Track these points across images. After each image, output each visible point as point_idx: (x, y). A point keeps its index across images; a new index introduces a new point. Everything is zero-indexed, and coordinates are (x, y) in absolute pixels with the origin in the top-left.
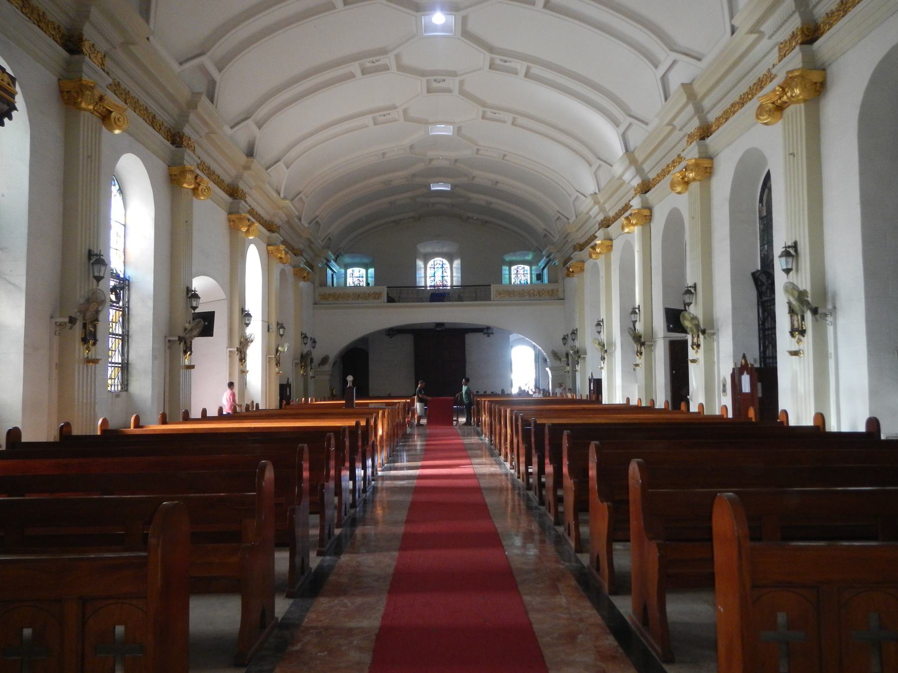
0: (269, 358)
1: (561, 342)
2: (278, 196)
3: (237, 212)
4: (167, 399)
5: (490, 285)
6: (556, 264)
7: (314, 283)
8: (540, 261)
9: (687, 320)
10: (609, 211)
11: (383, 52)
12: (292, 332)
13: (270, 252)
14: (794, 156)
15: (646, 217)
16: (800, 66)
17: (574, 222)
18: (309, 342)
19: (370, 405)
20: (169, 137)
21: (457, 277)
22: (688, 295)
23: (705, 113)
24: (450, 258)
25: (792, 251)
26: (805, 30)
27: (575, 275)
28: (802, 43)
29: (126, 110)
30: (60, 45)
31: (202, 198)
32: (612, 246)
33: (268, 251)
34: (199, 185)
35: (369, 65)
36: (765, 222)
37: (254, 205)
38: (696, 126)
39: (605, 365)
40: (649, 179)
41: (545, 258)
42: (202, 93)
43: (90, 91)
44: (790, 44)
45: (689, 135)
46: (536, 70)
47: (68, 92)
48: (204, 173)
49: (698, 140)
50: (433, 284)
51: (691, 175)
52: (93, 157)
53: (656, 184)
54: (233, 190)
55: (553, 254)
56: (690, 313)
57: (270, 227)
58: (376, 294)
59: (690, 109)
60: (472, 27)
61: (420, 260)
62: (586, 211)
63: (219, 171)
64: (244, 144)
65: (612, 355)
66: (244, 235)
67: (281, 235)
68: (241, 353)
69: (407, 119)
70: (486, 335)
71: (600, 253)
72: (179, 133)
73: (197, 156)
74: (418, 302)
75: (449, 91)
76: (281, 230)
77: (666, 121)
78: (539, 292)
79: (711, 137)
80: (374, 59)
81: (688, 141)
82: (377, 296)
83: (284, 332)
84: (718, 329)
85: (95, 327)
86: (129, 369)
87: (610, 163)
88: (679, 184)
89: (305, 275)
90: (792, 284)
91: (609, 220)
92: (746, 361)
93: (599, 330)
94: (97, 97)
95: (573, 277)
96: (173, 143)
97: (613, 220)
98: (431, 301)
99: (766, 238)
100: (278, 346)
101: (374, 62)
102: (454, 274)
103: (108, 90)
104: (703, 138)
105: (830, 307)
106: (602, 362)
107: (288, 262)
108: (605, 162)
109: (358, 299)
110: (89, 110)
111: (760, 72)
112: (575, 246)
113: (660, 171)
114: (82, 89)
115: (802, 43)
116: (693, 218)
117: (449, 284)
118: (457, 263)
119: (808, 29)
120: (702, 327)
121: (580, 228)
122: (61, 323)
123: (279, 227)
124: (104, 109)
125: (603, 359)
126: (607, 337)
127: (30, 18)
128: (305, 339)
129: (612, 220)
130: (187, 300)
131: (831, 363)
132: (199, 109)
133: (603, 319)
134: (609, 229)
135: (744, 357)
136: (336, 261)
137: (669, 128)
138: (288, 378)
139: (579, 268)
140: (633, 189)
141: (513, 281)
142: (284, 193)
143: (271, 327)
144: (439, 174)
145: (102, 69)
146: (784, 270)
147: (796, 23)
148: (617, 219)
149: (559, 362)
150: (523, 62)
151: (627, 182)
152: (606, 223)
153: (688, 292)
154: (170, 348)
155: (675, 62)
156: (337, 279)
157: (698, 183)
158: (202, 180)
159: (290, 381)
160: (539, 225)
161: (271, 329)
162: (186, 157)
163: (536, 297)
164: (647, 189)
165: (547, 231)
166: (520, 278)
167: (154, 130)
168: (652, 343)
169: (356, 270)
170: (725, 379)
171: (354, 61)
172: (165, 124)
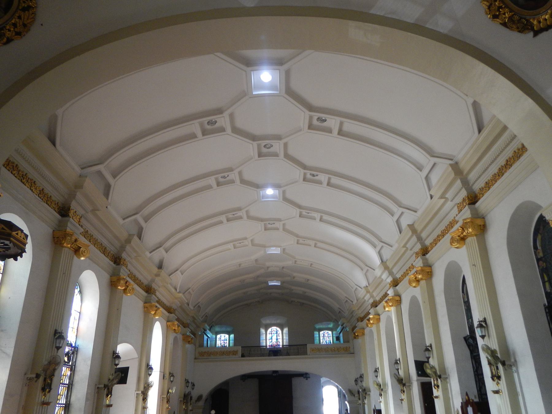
0: (163, 397)
1: (354, 383)
3: (150, 302)
5: (306, 345)
6: (348, 330)
7: (195, 345)
8: (338, 328)
9: (428, 369)
10: (376, 297)
12: (179, 379)
13: (169, 326)
14: (475, 266)
15: (398, 301)
16: (470, 216)
17: (356, 304)
18: (190, 385)
20: (113, 259)
21: (287, 339)
25: (484, 324)
26: (470, 197)
28: (469, 204)
29: (89, 246)
30: (57, 213)
31: (129, 295)
32: (380, 319)
33: (167, 325)
34: (128, 287)
36: (467, 305)
39: (382, 399)
41: (340, 326)
42: (135, 234)
43: (70, 237)
44: (463, 204)
45: (416, 253)
46: (325, 217)
47: (57, 238)
48: (131, 279)
49: (421, 256)
50: (271, 344)
51: (420, 277)
52: (66, 274)
53: (401, 281)
54: (148, 289)
55: (345, 324)
56: (429, 364)
57: (169, 310)
59: (414, 239)
60: (289, 196)
61: (263, 328)
62: (362, 297)
63: (140, 277)
64: (157, 260)
65: (386, 392)
66: (153, 316)
67: (176, 315)
68: (144, 394)
69: (253, 245)
70: (305, 378)
71: (373, 324)
72: (119, 257)
73: (128, 270)
74: (261, 356)
75: (277, 229)
76: (176, 312)
77: (402, 245)
80: (234, 213)
83: (173, 379)
84: (449, 375)
85: (51, 380)
86: (70, 408)
87: (373, 268)
88: (414, 281)
89: (190, 340)
90: (486, 345)
92: (468, 397)
93: (377, 375)
94: (73, 240)
95: (358, 338)
96: (114, 263)
97: (379, 303)
98: (269, 356)
100: (169, 389)
101: (234, 215)
102: (284, 338)
103: (80, 235)
104: (424, 255)
105: (513, 360)
106: (380, 397)
107: (180, 332)
109: (223, 355)
110: (68, 247)
111: (450, 218)
114: (65, 235)
115: (469, 204)
117: (281, 344)
118: (286, 330)
119: (471, 196)
120: (438, 373)
121: (361, 307)
122: (30, 378)
123: (175, 310)
124: (77, 246)
125: (381, 395)
126: (382, 380)
127: (42, 200)
128: (188, 383)
129: (378, 303)
131: (520, 398)
132: (132, 243)
133: (378, 368)
135: (467, 394)
136: (210, 330)
137: (405, 249)
138: (174, 412)
139: (361, 333)
141: (321, 341)
143: (165, 376)
144: (274, 275)
145: (79, 224)
146: (480, 336)
147: (464, 193)
148: (381, 302)
149: (353, 397)
150: (318, 213)
152: (375, 305)
153: (427, 350)
154: (98, 393)
155: (402, 213)
157: (424, 281)
158: (130, 283)
160: (336, 306)
161: (165, 377)
162: (122, 270)
164: (396, 284)
165: (340, 309)
166: (326, 340)
168: (410, 384)
169: (223, 335)
170: (458, 410)
172: (112, 252)
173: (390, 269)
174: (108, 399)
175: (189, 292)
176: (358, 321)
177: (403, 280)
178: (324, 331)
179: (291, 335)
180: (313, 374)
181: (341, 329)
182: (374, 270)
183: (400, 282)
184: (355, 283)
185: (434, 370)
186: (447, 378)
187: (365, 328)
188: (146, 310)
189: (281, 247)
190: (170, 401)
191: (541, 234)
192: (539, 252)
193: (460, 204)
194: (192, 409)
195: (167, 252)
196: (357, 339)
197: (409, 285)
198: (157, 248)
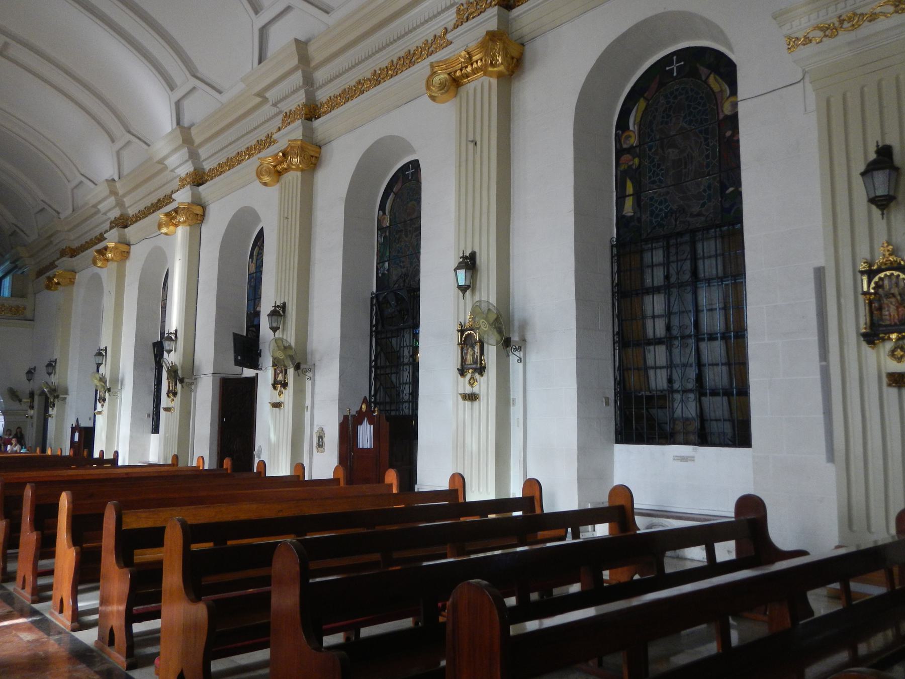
10: (128, 207)
14: (476, 144)
17: (66, 218)
22: (274, 318)
23: (315, 88)
27: (60, 288)
32: (128, 253)
36: (387, 234)
38: (300, 103)
40: (204, 169)
41: (8, 263)
49: (303, 118)
51: (296, 160)
53: (215, 176)
62: (93, 202)
71: (112, 260)
79: (318, 120)
84: (315, 364)
88: (269, 173)
91: (127, 220)
95: (56, 289)
97: (134, 220)
99: (388, 254)
112: (63, 249)
113: (224, 160)
129: (132, 220)
133: (106, 348)
134: (126, 229)
137: (259, 99)
139: (68, 280)
140: (178, 179)
146: (459, 287)
149: (18, 402)
164: (200, 182)
165: (16, 226)
168: (192, 382)
173: (195, 145)
176: (63, 253)
182: (149, 145)
183: (212, 179)
184: (79, 171)
185: (291, 353)
186: (305, 371)
187: (76, 271)
191: (646, 99)
192: (629, 137)
193: (465, 6)
197: (256, 177)
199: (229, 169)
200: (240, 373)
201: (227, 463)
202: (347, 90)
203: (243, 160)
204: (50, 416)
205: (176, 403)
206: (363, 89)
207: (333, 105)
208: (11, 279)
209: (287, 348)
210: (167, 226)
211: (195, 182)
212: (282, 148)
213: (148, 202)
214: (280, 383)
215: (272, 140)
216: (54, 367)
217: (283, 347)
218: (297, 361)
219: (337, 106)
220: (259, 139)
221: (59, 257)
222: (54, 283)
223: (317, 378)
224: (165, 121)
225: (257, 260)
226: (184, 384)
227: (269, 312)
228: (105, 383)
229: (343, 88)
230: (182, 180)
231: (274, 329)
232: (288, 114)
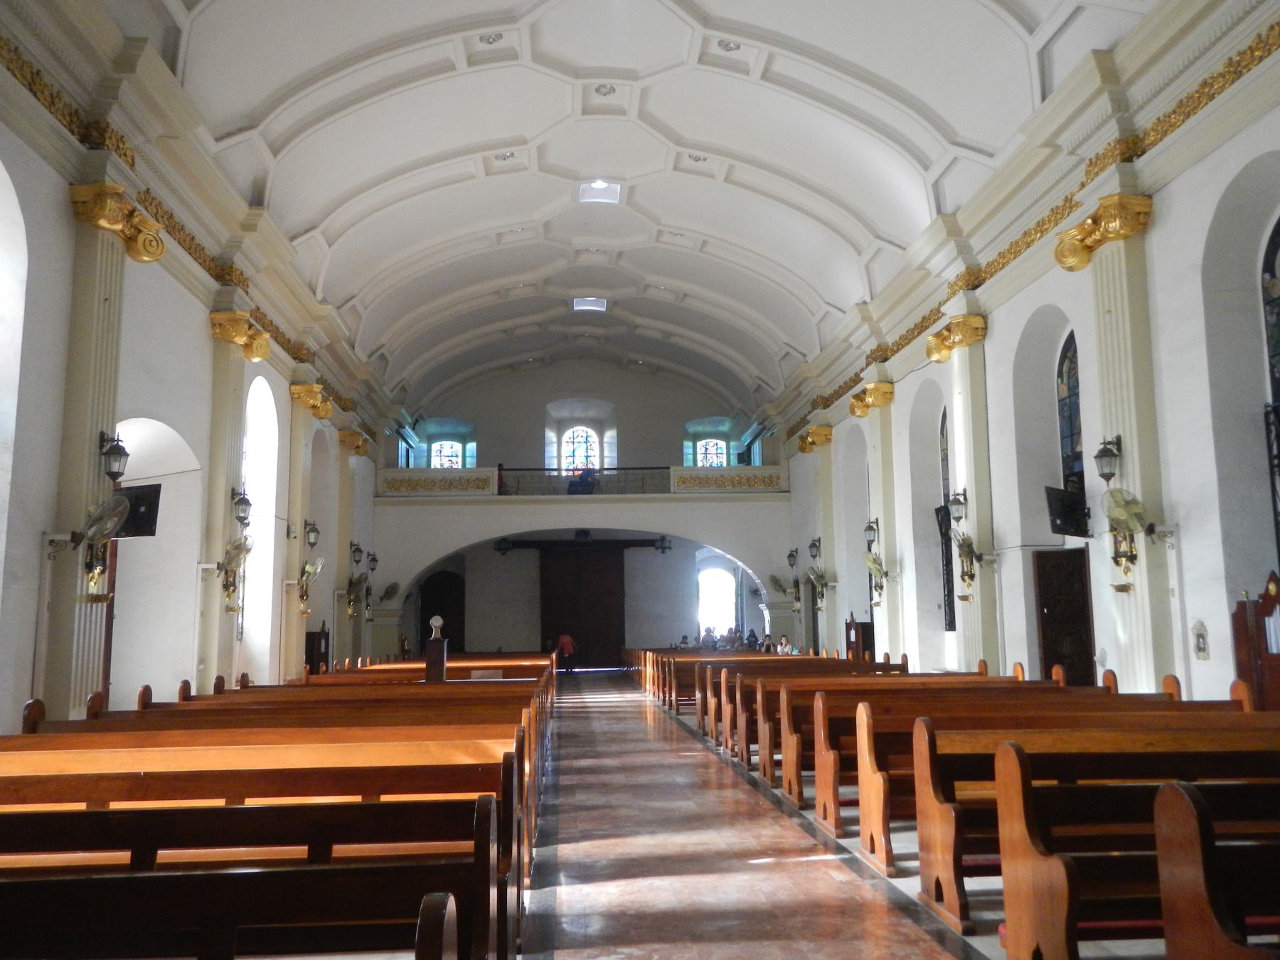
0: (288, 585)
1: (787, 562)
2: (312, 295)
3: (230, 310)
4: (42, 665)
5: (669, 468)
6: (775, 435)
7: (375, 462)
8: (743, 432)
10: (887, 333)
11: (509, 17)
13: (296, 396)
17: (816, 358)
19: (473, 673)
20: (74, 126)
22: (1106, 460)
23: (1132, 111)
24: (600, 427)
27: (815, 448)
31: (146, 258)
32: (892, 393)
33: (292, 394)
34: (140, 231)
35: (482, 47)
37: (266, 308)
40: (979, 265)
41: (755, 425)
42: (145, 40)
49: (1118, 161)
50: (571, 467)
51: (1115, 225)
53: (996, 271)
57: (298, 352)
58: (480, 480)
59: (1104, 103)
61: (552, 429)
62: (845, 334)
64: (245, 179)
66: (243, 354)
68: (226, 572)
69: (544, 168)
70: (660, 550)
71: (873, 405)
72: (97, 122)
74: (549, 493)
75: (622, 112)
76: (317, 362)
78: (748, 480)
81: (1088, 172)
82: (481, 484)
83: (317, 538)
84: (1177, 525)
88: (1074, 251)
89: (360, 443)
91: (886, 351)
96: (82, 141)
97: (895, 349)
100: (306, 564)
101: (490, 43)
102: (606, 453)
107: (330, 415)
108: (890, 242)
109: (449, 488)
112: (814, 400)
113: (1007, 246)
116: (1109, 312)
118: (610, 435)
126: (886, 548)
130: (100, 459)
132: (138, 69)
133: (877, 519)
134: (886, 363)
137: (1047, 151)
138: (324, 622)
141: (700, 464)
142: (323, 291)
143: (293, 528)
144: (589, 280)
149: (782, 594)
151: (934, 274)
152: (882, 355)
156: (415, 458)
158: (143, 221)
159: (327, 627)
160: (747, 371)
162: (110, 170)
163: (744, 487)
164: (976, 283)
166: (711, 461)
167: (36, 100)
171: (455, 32)
172: (66, 99)
174: (93, 577)
175: (354, 306)
177: (1003, 268)
178: (708, 440)
179: (623, 446)
180: (680, 538)
181: (757, 432)
182: (904, 249)
183: (991, 276)
184: (823, 299)
185: (1137, 510)
186: (1163, 536)
188: (220, 333)
189: (624, 180)
190: (309, 592)
194: (371, 618)
195: (275, 153)
196: (808, 452)
197: (1056, 262)
198: (241, 130)
199: (1015, 258)
200: (1062, 543)
201: (1057, 673)
202: (1185, 101)
203: (1033, 241)
204: (819, 609)
205: (974, 589)
206: (1212, 91)
207: (1165, 128)
208: (760, 444)
209: (1129, 503)
210: (938, 350)
211: (969, 285)
212: (1092, 211)
213: (910, 323)
214: (1124, 555)
215: (1073, 203)
216: (818, 548)
217: (1123, 503)
218: (1148, 522)
219: (1171, 129)
220: (1053, 206)
221: (810, 410)
222: (808, 443)
223: (1185, 545)
224: (921, 211)
225: (1069, 378)
226: (982, 563)
227: (1095, 453)
228: (880, 565)
229: (1177, 100)
230: (951, 285)
231: (1107, 477)
232: (1094, 160)
